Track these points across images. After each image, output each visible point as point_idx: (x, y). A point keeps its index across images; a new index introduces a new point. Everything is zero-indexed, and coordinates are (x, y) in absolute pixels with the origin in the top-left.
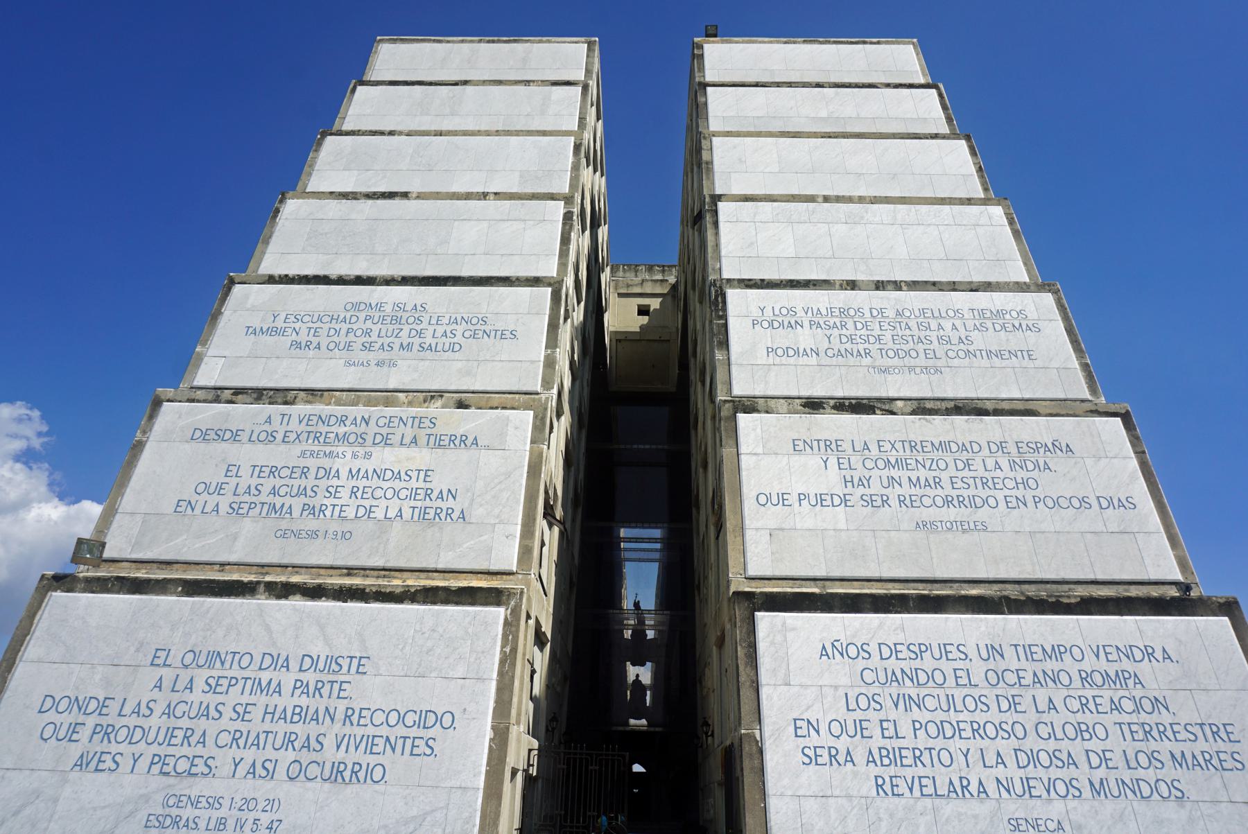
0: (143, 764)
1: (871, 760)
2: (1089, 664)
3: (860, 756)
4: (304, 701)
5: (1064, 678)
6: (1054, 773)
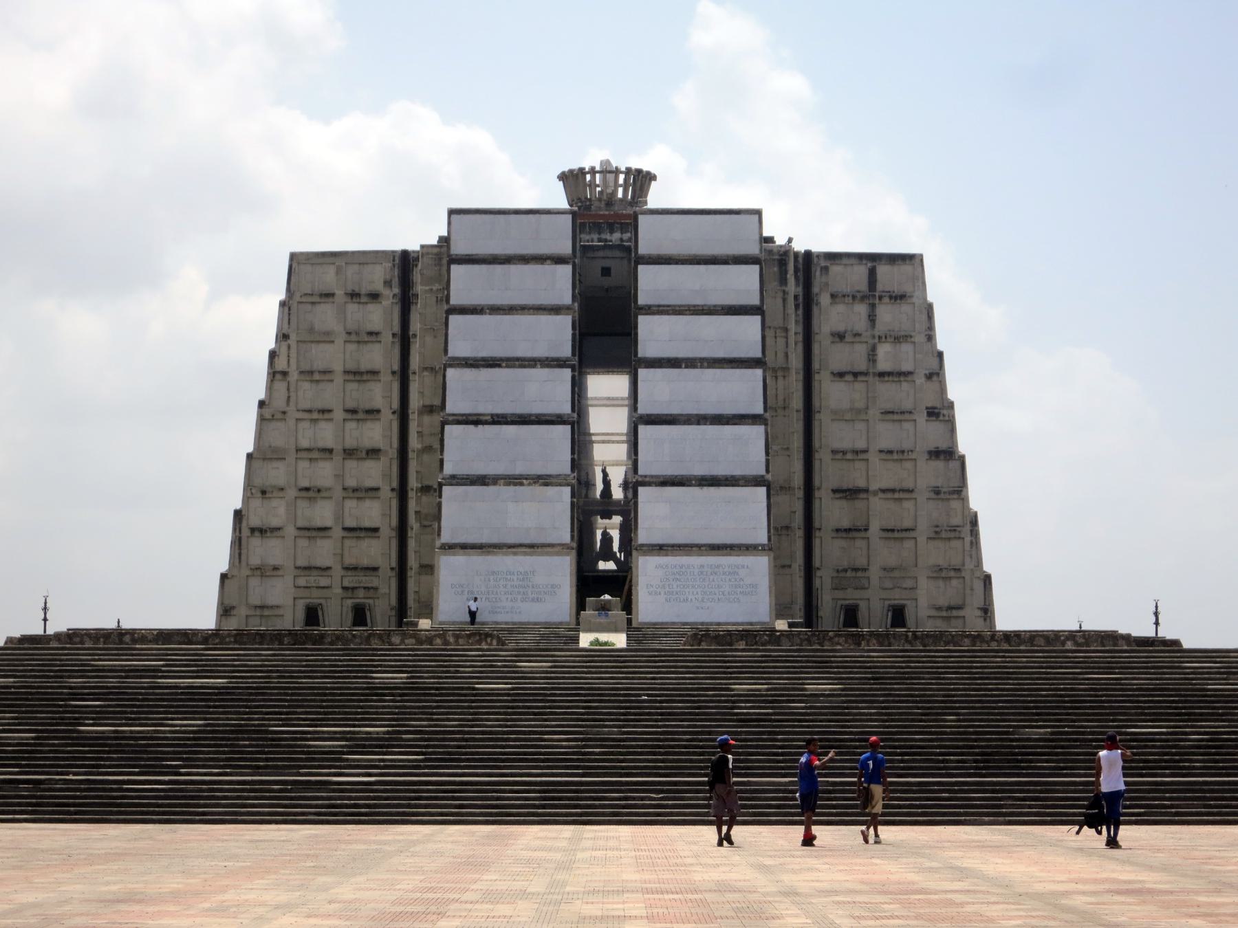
0: (484, 599)
1: (665, 593)
2: (726, 570)
3: (662, 593)
4: (521, 583)
5: (718, 574)
6: (710, 596)
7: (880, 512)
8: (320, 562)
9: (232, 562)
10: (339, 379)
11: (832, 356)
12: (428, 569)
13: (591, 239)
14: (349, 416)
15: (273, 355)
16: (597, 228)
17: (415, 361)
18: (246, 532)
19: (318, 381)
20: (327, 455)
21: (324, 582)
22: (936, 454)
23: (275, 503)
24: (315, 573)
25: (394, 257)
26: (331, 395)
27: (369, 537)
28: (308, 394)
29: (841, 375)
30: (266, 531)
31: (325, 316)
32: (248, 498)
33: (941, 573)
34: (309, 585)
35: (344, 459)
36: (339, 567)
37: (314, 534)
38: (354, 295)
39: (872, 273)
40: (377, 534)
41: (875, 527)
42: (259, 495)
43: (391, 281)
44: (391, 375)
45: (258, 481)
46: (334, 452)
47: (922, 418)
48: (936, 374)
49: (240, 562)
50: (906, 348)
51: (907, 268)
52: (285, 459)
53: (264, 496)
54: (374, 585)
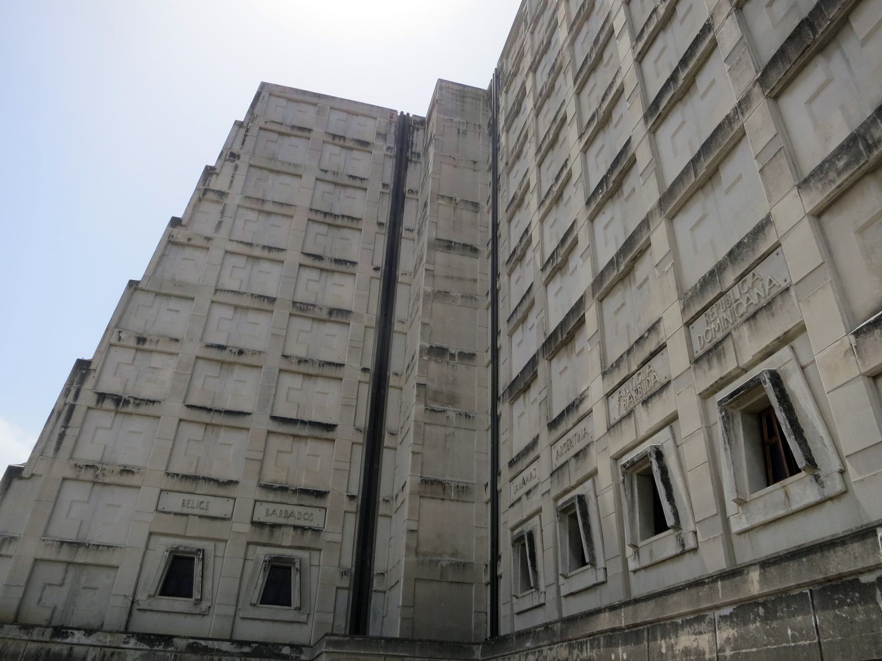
9: (40, 447)
10: (301, 217)
14: (309, 261)
15: (209, 172)
18: (87, 397)
19: (269, 213)
20: (266, 305)
21: (217, 507)
23: (157, 360)
24: (204, 488)
25: (391, 117)
27: (316, 438)
30: (127, 402)
32: (111, 345)
34: (185, 510)
35: (291, 315)
36: (254, 483)
37: (217, 419)
40: (330, 435)
42: (133, 343)
43: (386, 134)
44: (376, 225)
45: (136, 324)
46: (277, 303)
49: (57, 449)
52: (193, 299)
53: (140, 346)
54: (313, 524)
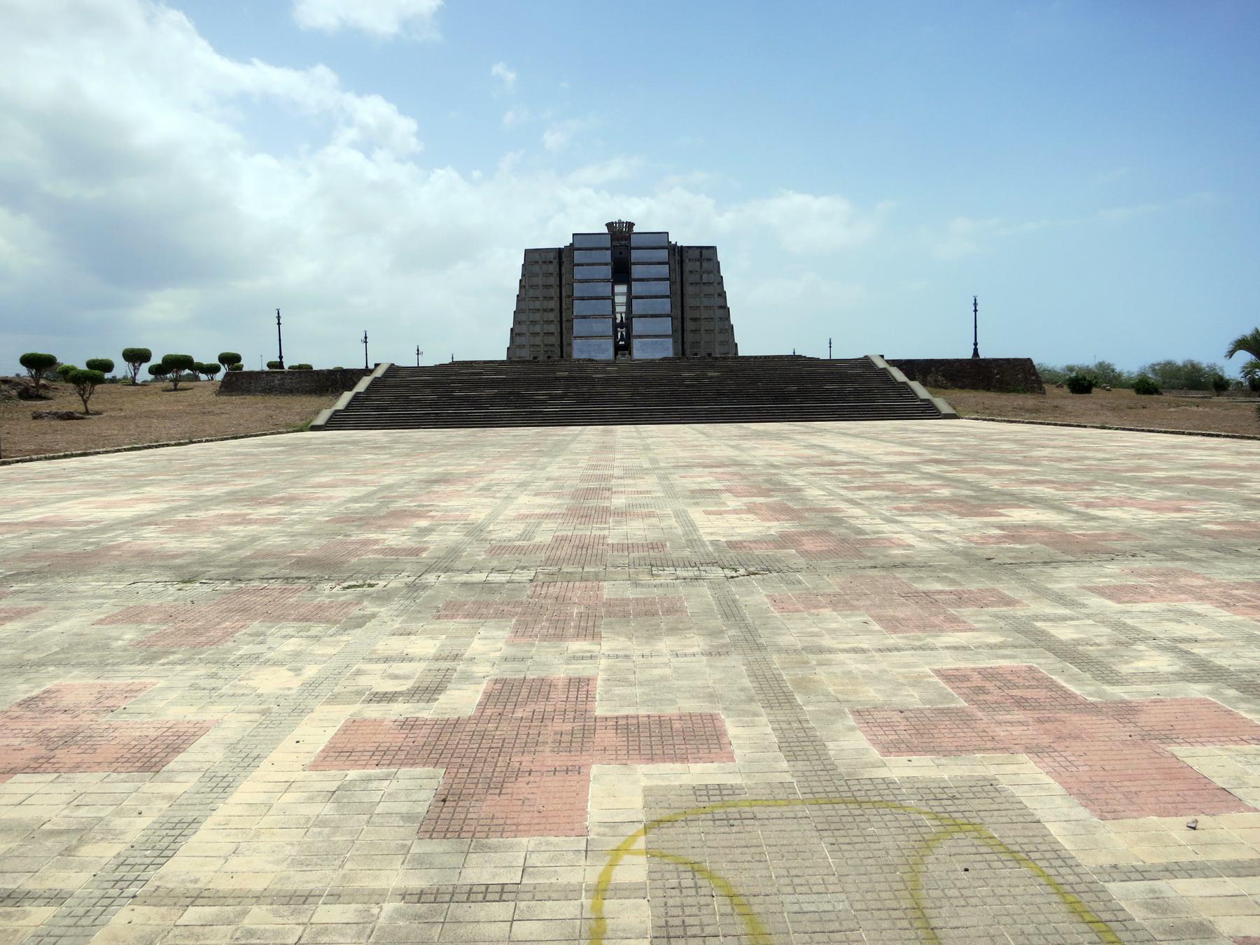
7: (704, 325)
8: (537, 343)
10: (541, 288)
11: (689, 278)
12: (570, 345)
13: (614, 243)
15: (520, 281)
16: (618, 240)
17: (564, 282)
22: (721, 307)
26: (538, 293)
28: (531, 293)
29: (692, 284)
31: (536, 269)
33: (722, 343)
38: (545, 262)
39: (701, 252)
41: (702, 330)
47: (716, 296)
48: (721, 283)
50: (712, 275)
51: (712, 251)
